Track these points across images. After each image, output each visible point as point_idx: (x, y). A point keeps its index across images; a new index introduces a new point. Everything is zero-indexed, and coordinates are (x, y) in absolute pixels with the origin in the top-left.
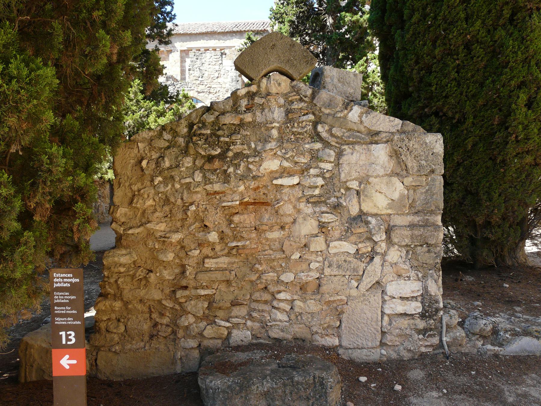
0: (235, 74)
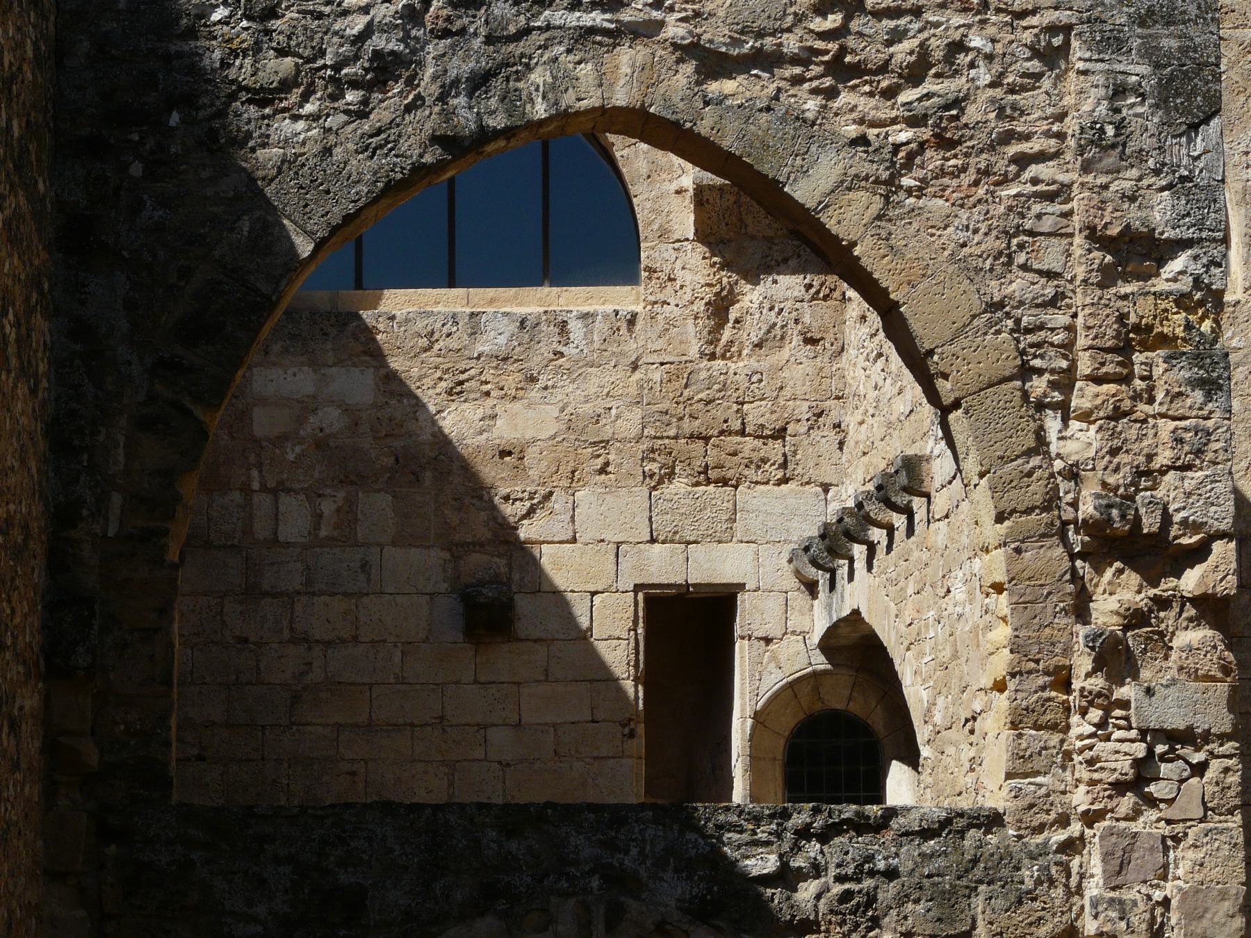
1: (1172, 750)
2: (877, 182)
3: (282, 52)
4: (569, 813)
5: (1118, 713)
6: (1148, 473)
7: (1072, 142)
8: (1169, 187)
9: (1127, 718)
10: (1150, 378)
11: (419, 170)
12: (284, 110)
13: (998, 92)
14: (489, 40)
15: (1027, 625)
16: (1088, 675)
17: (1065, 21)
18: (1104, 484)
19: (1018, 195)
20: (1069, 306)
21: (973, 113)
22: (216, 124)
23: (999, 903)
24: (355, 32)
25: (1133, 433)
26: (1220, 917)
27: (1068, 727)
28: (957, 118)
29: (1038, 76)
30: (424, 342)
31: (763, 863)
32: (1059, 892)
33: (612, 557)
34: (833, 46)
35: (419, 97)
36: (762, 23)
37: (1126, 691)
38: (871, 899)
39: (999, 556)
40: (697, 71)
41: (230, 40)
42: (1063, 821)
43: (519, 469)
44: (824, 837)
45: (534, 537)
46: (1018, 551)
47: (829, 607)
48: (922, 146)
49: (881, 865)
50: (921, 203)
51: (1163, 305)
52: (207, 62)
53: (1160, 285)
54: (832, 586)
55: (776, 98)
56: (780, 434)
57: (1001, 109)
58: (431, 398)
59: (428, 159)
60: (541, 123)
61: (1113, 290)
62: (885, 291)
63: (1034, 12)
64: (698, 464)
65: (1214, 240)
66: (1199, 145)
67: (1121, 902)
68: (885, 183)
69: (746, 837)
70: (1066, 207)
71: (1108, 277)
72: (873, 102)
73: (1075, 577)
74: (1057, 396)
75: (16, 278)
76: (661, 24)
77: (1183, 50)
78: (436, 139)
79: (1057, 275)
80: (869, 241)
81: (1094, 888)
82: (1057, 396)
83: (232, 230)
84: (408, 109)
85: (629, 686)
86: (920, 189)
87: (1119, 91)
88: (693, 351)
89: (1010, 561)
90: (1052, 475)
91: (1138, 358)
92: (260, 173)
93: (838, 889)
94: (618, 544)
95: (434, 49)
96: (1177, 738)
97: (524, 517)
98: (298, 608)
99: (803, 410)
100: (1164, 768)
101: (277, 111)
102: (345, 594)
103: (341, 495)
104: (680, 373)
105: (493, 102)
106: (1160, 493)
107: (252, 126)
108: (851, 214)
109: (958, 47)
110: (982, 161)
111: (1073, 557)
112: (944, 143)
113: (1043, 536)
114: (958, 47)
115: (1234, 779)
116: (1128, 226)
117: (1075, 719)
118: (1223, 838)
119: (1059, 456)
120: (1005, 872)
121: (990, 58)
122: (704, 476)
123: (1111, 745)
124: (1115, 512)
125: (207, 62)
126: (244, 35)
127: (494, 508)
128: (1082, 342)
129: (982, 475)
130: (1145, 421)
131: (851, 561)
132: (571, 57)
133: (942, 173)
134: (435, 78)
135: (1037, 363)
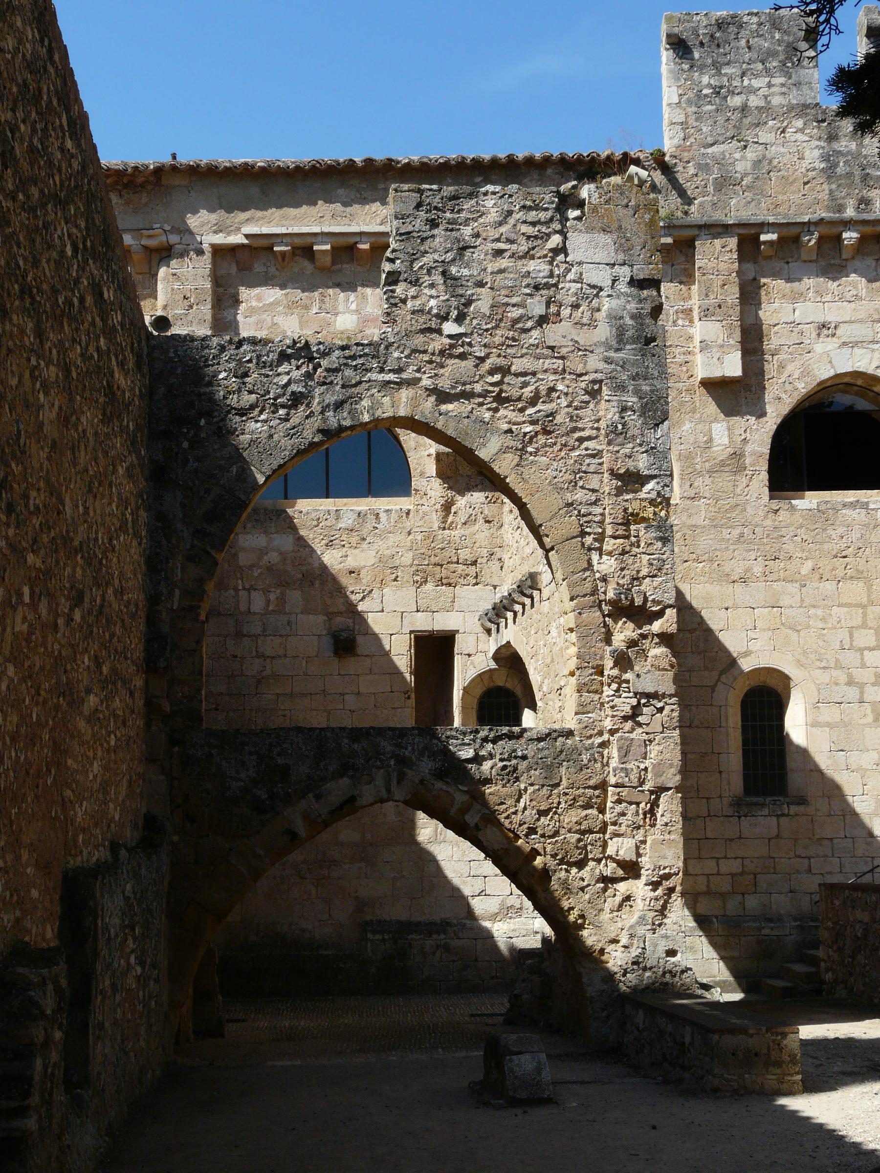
0: (632, 306)
1: (648, 701)
2: (516, 449)
3: (250, 392)
4: (381, 731)
5: (624, 685)
6: (637, 579)
7: (603, 432)
8: (646, 451)
9: (628, 688)
10: (638, 536)
11: (312, 445)
12: (252, 418)
13: (570, 410)
14: (343, 386)
15: (584, 647)
16: (611, 669)
17: (600, 378)
18: (618, 584)
19: (580, 455)
20: (602, 505)
21: (559, 419)
22: (221, 424)
23: (572, 770)
24: (283, 383)
25: (630, 561)
26: (670, 776)
27: (602, 692)
28: (552, 421)
29: (588, 402)
30: (315, 523)
31: (467, 753)
32: (599, 765)
33: (400, 619)
34: (497, 389)
35: (312, 412)
36: (465, 379)
37: (628, 676)
38: (515, 769)
39: (572, 615)
40: (436, 400)
41: (227, 387)
42: (600, 733)
43: (358, 579)
44: (494, 741)
45: (365, 609)
46: (580, 613)
47: (496, 640)
48: (537, 433)
49: (520, 754)
50: (536, 459)
51: (644, 504)
52: (217, 397)
53: (642, 495)
54: (498, 631)
55: (472, 412)
56: (474, 563)
57: (572, 417)
58: (318, 547)
59: (316, 440)
60: (367, 423)
61: (621, 497)
62: (520, 498)
63: (586, 374)
64: (438, 577)
65: (666, 475)
66: (659, 433)
67: (626, 769)
68: (520, 450)
69: (459, 741)
70: (600, 461)
71: (619, 492)
72: (514, 414)
73: (605, 625)
74: (597, 545)
75: (132, 493)
76: (420, 379)
77: (652, 391)
78: (319, 431)
79: (597, 491)
80: (513, 476)
81: (614, 763)
82: (597, 545)
83: (228, 471)
84: (307, 417)
85: (407, 676)
86: (536, 452)
87: (624, 409)
88: (436, 526)
89: (576, 618)
90: (595, 580)
91: (632, 527)
92: (241, 446)
93: (501, 764)
94: (402, 613)
95: (318, 391)
96: (649, 696)
97: (360, 601)
98: (260, 642)
99: (485, 552)
100: (645, 710)
101: (248, 419)
102: (280, 636)
103: (278, 591)
104: (430, 536)
105: (345, 414)
106: (642, 588)
107: (237, 425)
108: (505, 464)
109: (552, 389)
110: (563, 440)
111: (604, 616)
112: (546, 432)
113: (591, 607)
114: (552, 389)
115: (676, 714)
116: (628, 469)
117: (605, 688)
118: (671, 740)
119: (598, 571)
120: (575, 756)
121: (566, 394)
122: (441, 582)
123: (621, 700)
124: (623, 596)
125: (217, 397)
126: (234, 385)
127: (347, 597)
128: (608, 520)
129: (564, 580)
130: (636, 556)
131: (506, 619)
132: (380, 394)
133: (545, 445)
134: (319, 403)
135: (588, 530)
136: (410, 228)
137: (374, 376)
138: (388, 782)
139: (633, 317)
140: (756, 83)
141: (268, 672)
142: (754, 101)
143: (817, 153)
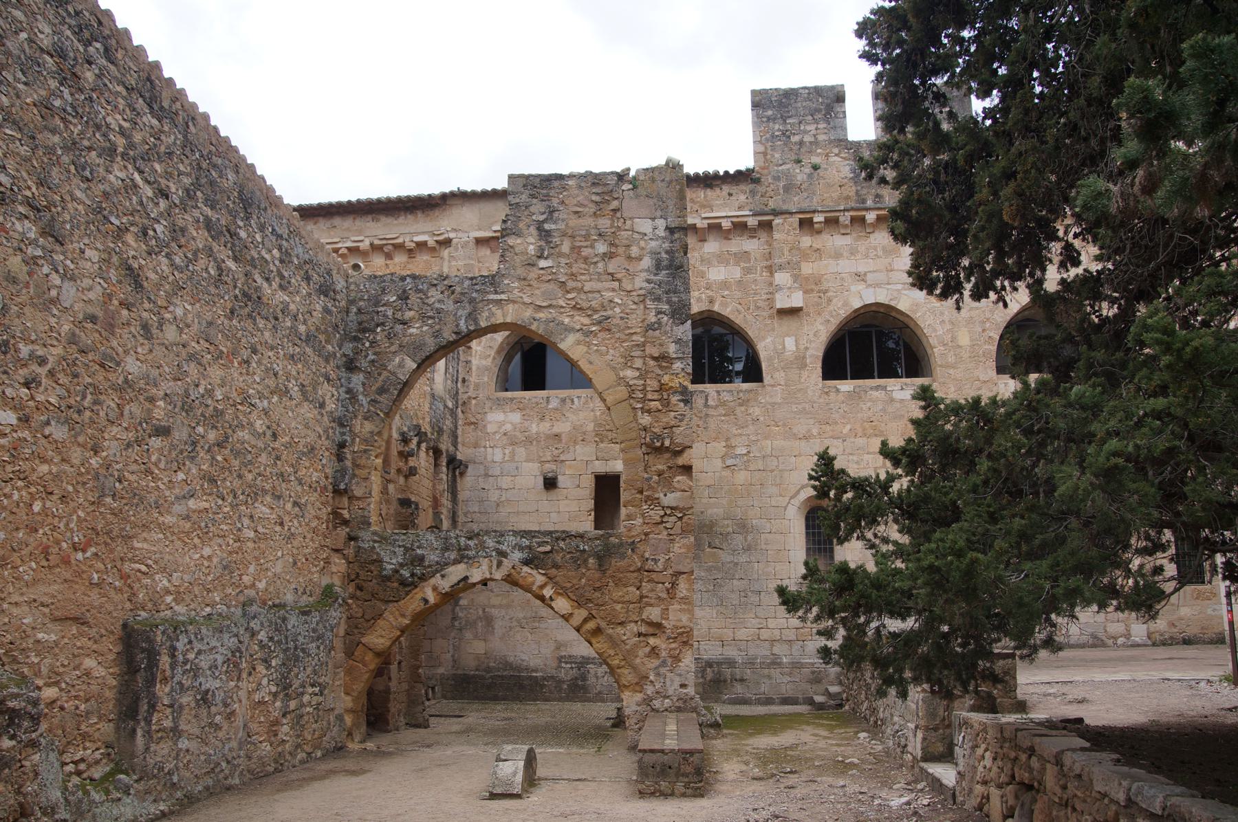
0: (666, 245)
77: (679, 301)
87: (659, 312)
136: (518, 201)
137: (492, 297)
138: (491, 567)
139: (667, 252)
140: (808, 128)
141: (503, 499)
142: (807, 139)
143: (848, 168)
